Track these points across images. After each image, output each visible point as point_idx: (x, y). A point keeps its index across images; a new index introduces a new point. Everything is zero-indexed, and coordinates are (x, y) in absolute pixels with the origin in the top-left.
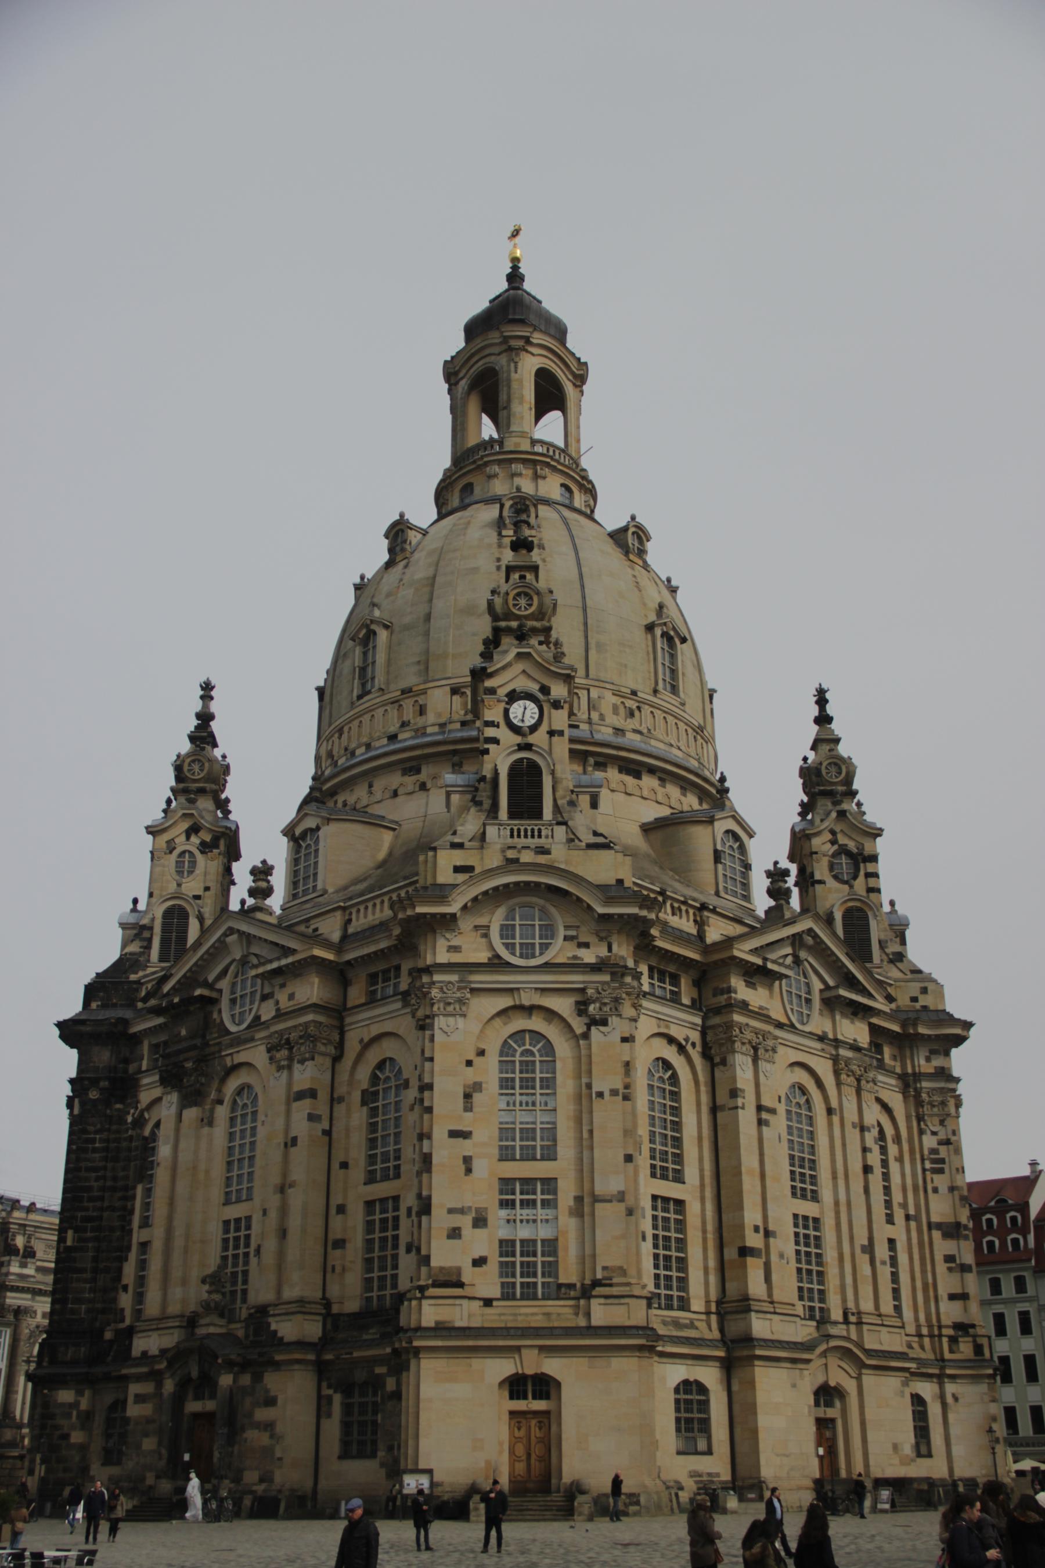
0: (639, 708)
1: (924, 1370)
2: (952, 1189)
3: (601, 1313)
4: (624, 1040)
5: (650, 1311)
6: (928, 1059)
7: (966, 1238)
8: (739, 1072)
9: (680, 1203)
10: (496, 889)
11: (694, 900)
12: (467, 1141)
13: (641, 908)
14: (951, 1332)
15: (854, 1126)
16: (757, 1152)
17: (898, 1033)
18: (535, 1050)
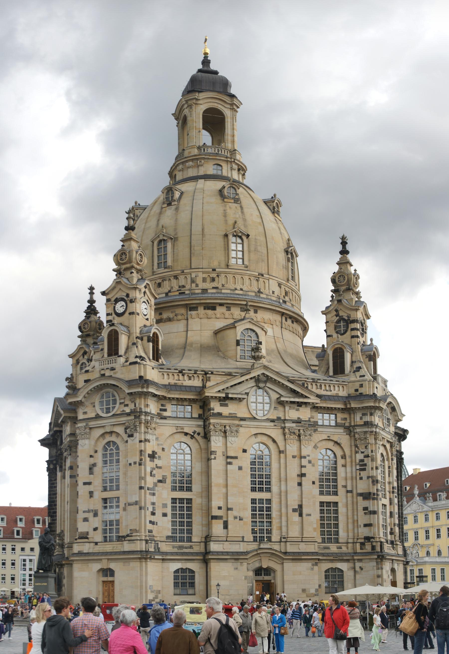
0: (218, 276)
1: (341, 558)
2: (368, 477)
3: (127, 546)
4: (141, 441)
5: (147, 545)
6: (361, 418)
7: (374, 499)
8: (213, 443)
9: (189, 501)
10: (94, 388)
11: (202, 371)
12: (90, 486)
13: (143, 387)
14: (363, 541)
15: (294, 457)
16: (225, 476)
17: (342, 408)
18: (114, 448)
